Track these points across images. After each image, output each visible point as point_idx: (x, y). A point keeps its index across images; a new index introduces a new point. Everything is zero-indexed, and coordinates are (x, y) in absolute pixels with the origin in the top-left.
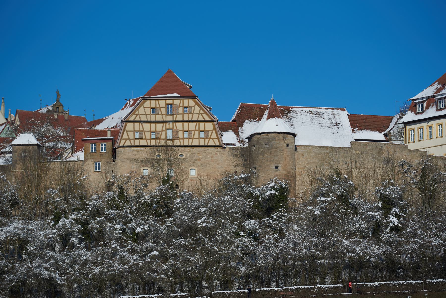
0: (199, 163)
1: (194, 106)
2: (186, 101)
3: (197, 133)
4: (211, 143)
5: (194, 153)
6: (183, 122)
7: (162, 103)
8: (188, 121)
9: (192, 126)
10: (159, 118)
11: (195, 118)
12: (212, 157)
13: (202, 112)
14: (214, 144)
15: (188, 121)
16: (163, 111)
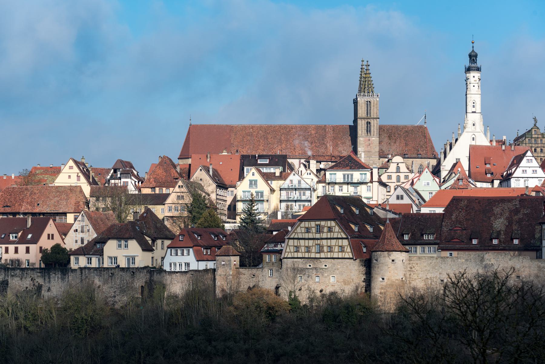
0: (337, 272)
1: (335, 227)
2: (329, 222)
3: (337, 247)
4: (347, 256)
5: (334, 264)
6: (327, 239)
7: (313, 224)
8: (331, 239)
9: (333, 242)
10: (311, 236)
11: (335, 236)
12: (347, 267)
13: (340, 231)
14: (348, 257)
15: (331, 239)
16: (314, 230)
